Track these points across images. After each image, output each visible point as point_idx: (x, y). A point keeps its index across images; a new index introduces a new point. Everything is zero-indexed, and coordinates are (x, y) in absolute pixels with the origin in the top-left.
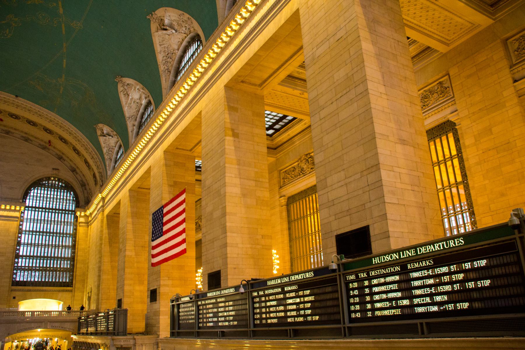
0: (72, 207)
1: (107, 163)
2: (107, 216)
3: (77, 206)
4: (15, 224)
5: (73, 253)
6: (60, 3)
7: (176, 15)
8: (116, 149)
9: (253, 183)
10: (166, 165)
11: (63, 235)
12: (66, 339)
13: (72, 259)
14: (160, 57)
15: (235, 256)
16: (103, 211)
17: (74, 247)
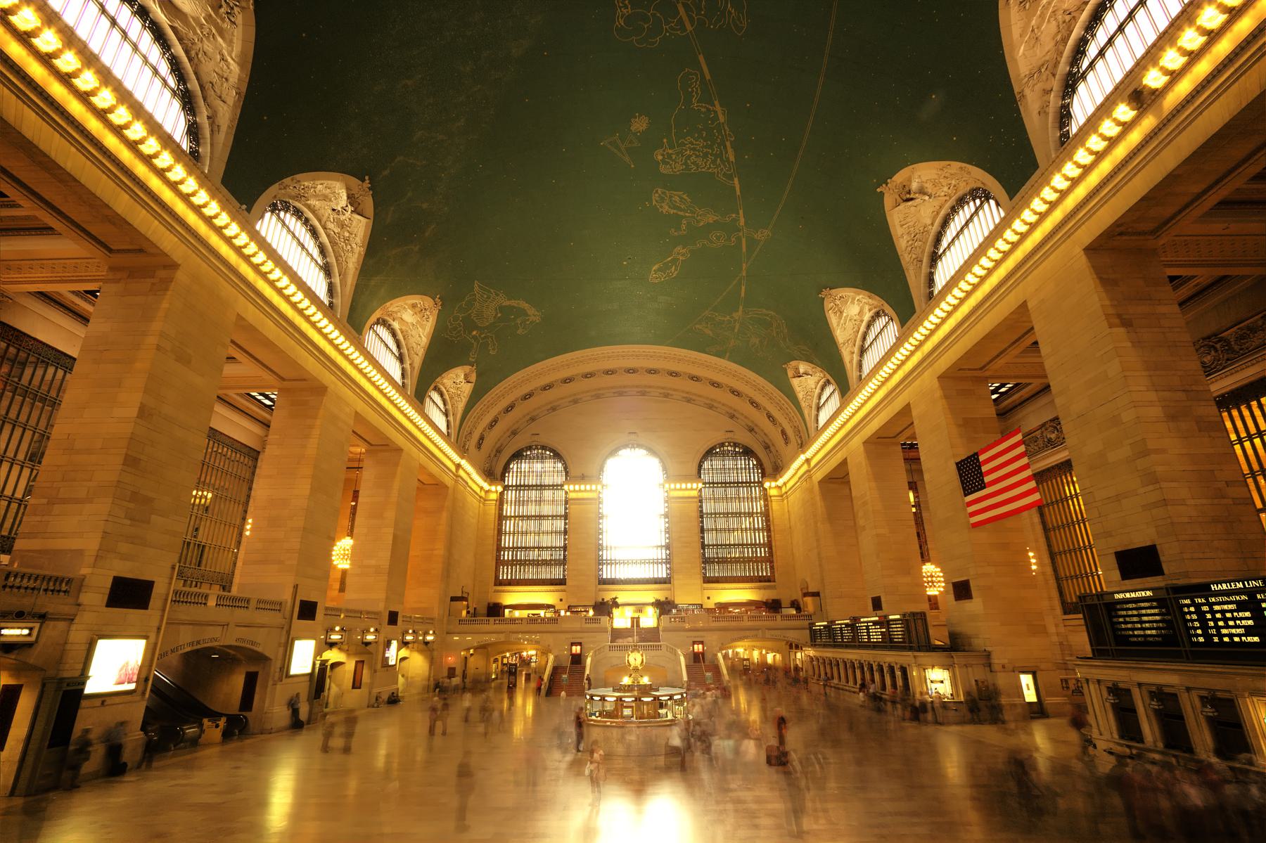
0: (756, 477)
1: (806, 412)
2: (820, 482)
3: (764, 475)
4: (695, 506)
5: (769, 537)
6: (741, 212)
7: (935, 171)
8: (818, 391)
9: (1182, 395)
10: (946, 397)
11: (750, 514)
12: (778, 651)
13: (769, 545)
14: (902, 243)
15: (1186, 520)
16: (810, 477)
17: (768, 529)
